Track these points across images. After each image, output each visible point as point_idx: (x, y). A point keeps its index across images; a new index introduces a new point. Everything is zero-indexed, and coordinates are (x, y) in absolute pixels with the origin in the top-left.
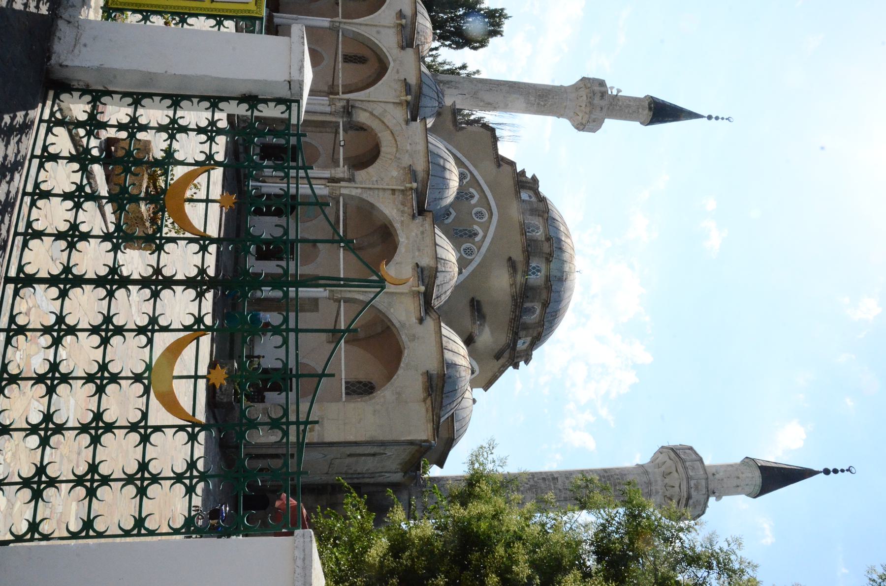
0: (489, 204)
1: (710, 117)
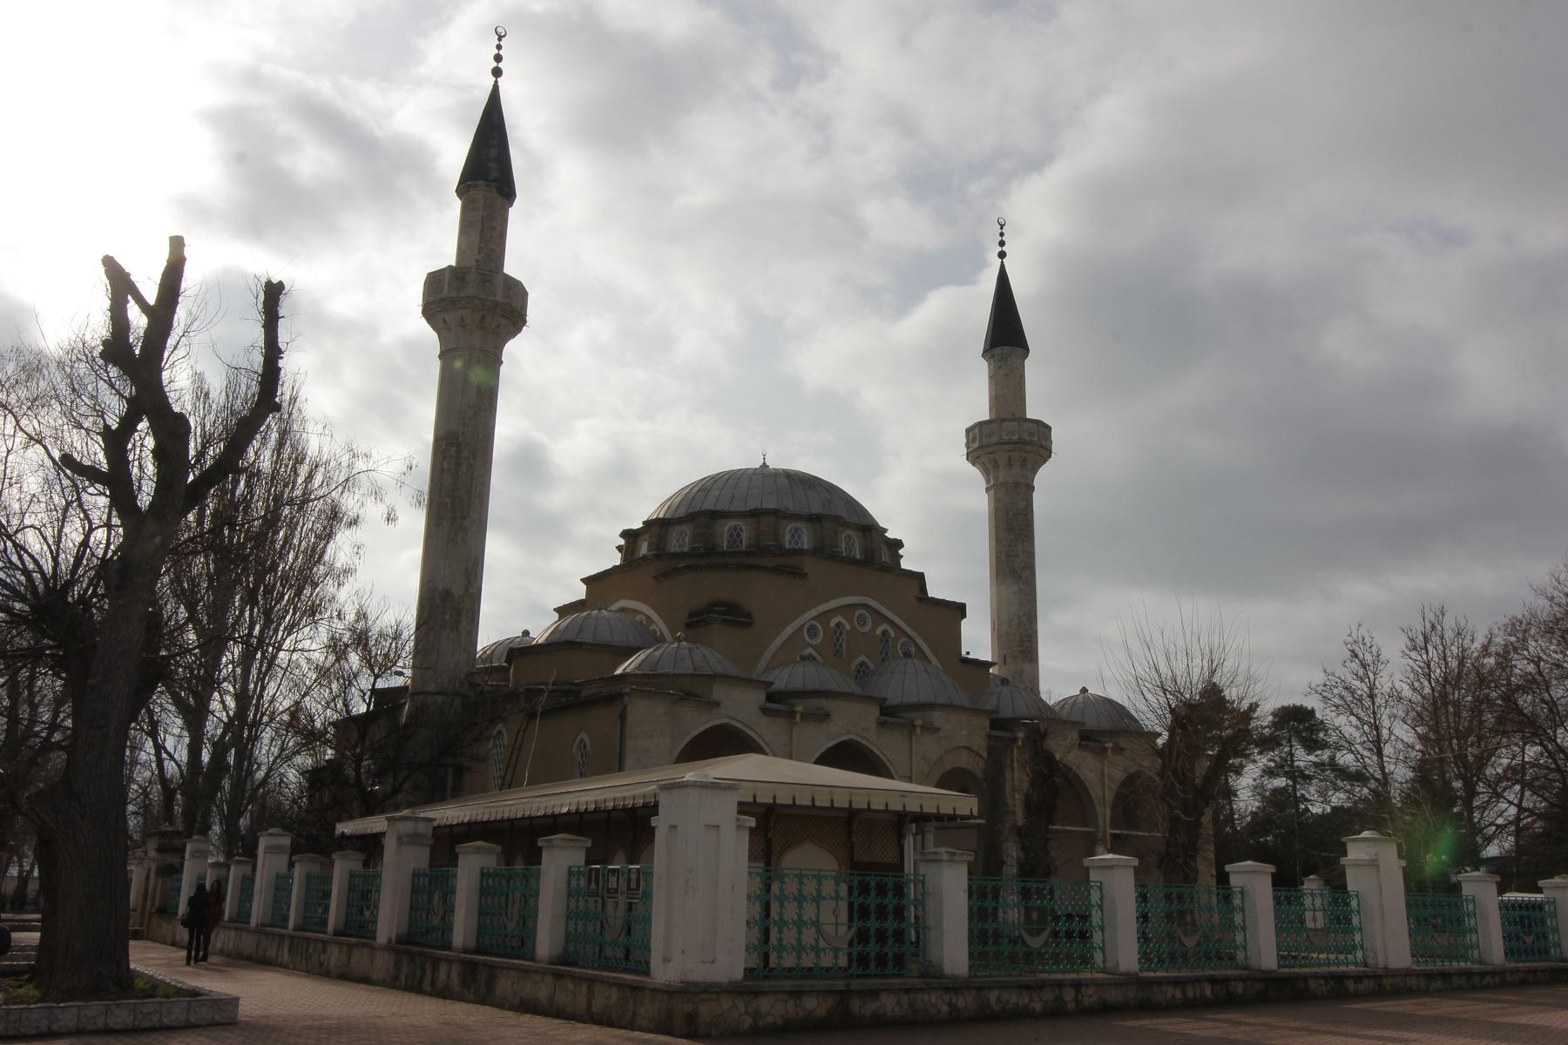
0: (850, 606)
1: (497, 72)
